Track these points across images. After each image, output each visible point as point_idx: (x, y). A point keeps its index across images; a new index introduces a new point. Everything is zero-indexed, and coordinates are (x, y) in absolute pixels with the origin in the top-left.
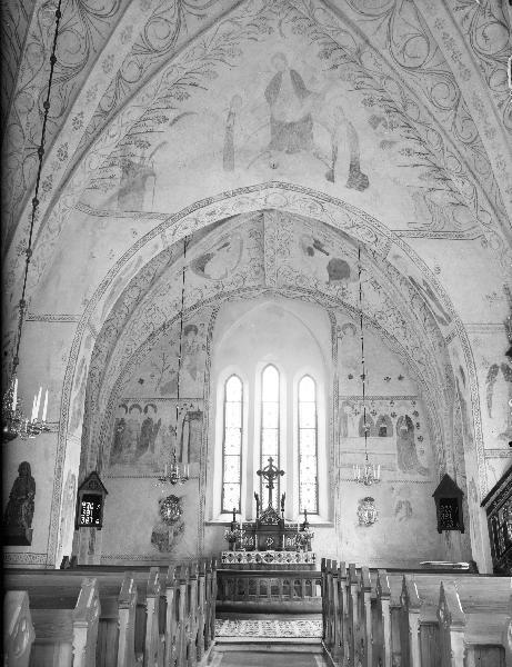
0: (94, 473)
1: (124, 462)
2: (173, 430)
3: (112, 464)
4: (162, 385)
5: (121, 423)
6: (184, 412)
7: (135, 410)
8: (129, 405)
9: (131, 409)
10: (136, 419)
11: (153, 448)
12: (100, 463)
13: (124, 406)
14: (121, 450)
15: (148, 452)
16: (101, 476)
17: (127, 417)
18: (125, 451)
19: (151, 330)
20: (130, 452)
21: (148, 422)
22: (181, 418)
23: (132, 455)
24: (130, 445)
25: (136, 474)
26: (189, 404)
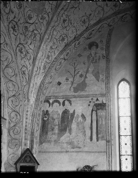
0: (28, 149)
1: (49, 142)
2: (83, 116)
3: (41, 143)
4: (75, 85)
5: (46, 113)
6: (92, 104)
7: (56, 104)
8: (51, 101)
9: (53, 103)
10: (57, 110)
11: (70, 130)
12: (32, 141)
13: (48, 102)
14: (47, 133)
15: (67, 134)
16: (34, 151)
17: (50, 110)
18: (50, 133)
19: (66, 41)
20: (54, 134)
21: (65, 112)
22: (91, 108)
23: (55, 137)
24: (53, 130)
25: (59, 149)
26: (95, 99)
